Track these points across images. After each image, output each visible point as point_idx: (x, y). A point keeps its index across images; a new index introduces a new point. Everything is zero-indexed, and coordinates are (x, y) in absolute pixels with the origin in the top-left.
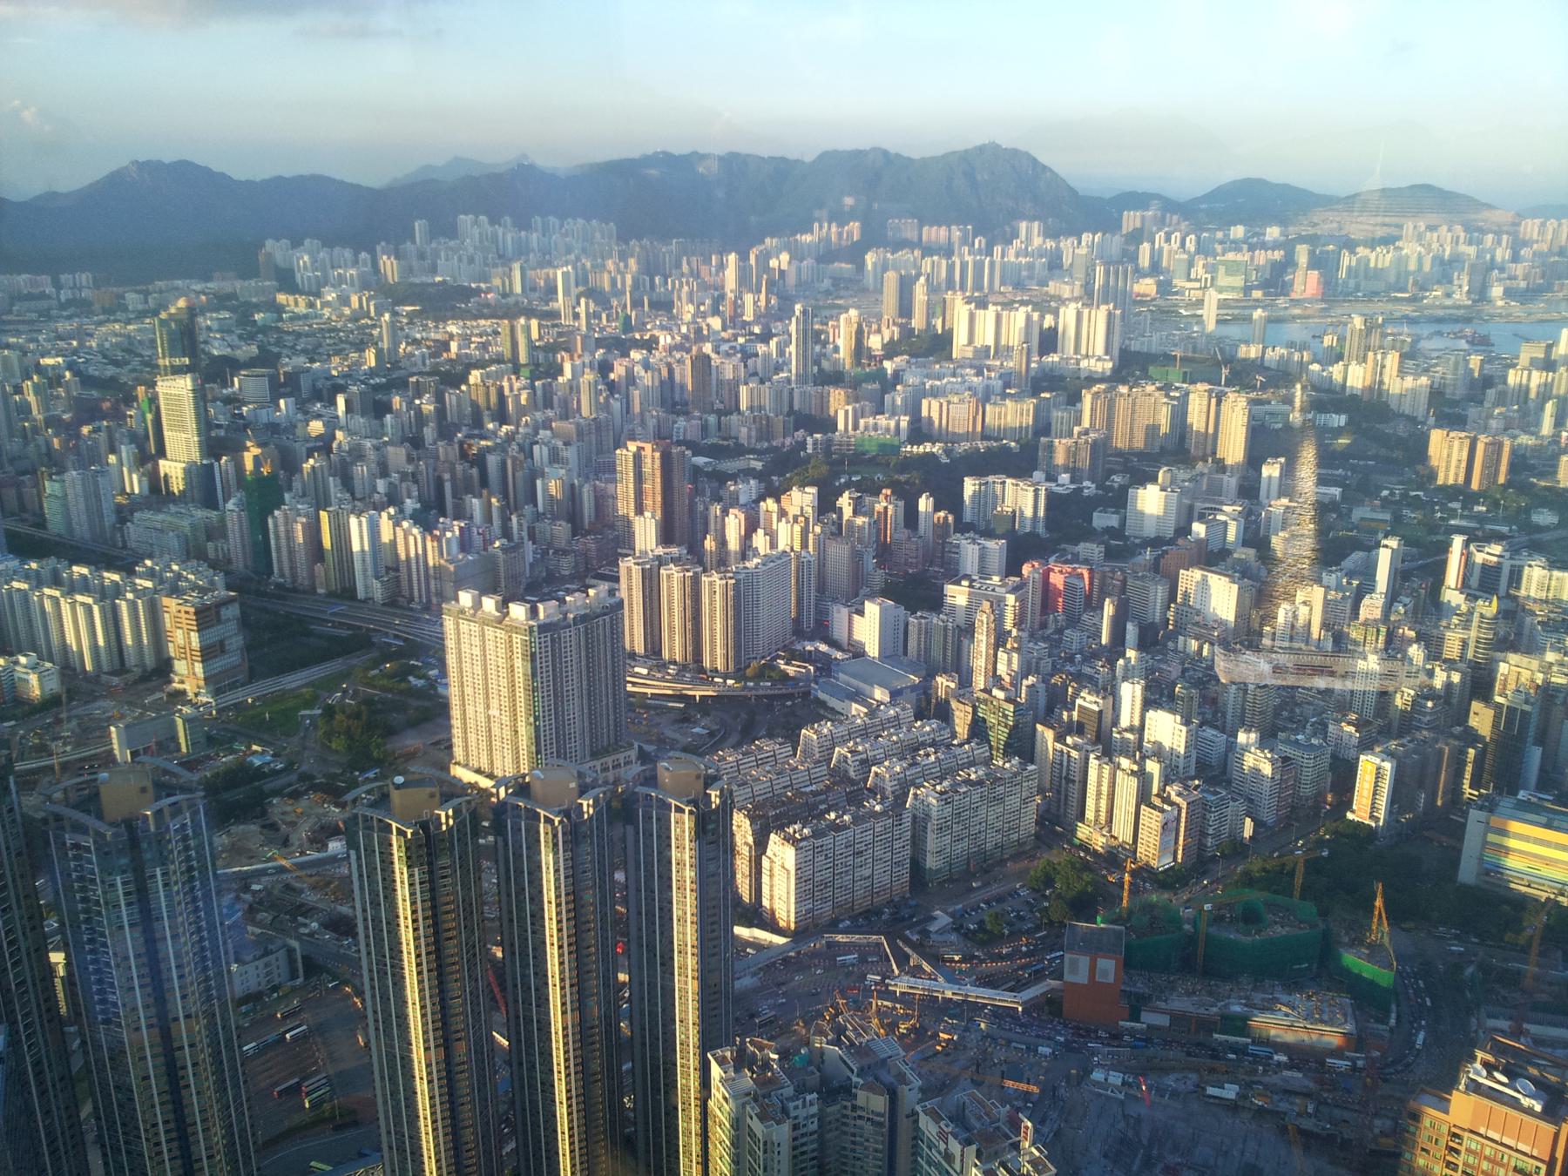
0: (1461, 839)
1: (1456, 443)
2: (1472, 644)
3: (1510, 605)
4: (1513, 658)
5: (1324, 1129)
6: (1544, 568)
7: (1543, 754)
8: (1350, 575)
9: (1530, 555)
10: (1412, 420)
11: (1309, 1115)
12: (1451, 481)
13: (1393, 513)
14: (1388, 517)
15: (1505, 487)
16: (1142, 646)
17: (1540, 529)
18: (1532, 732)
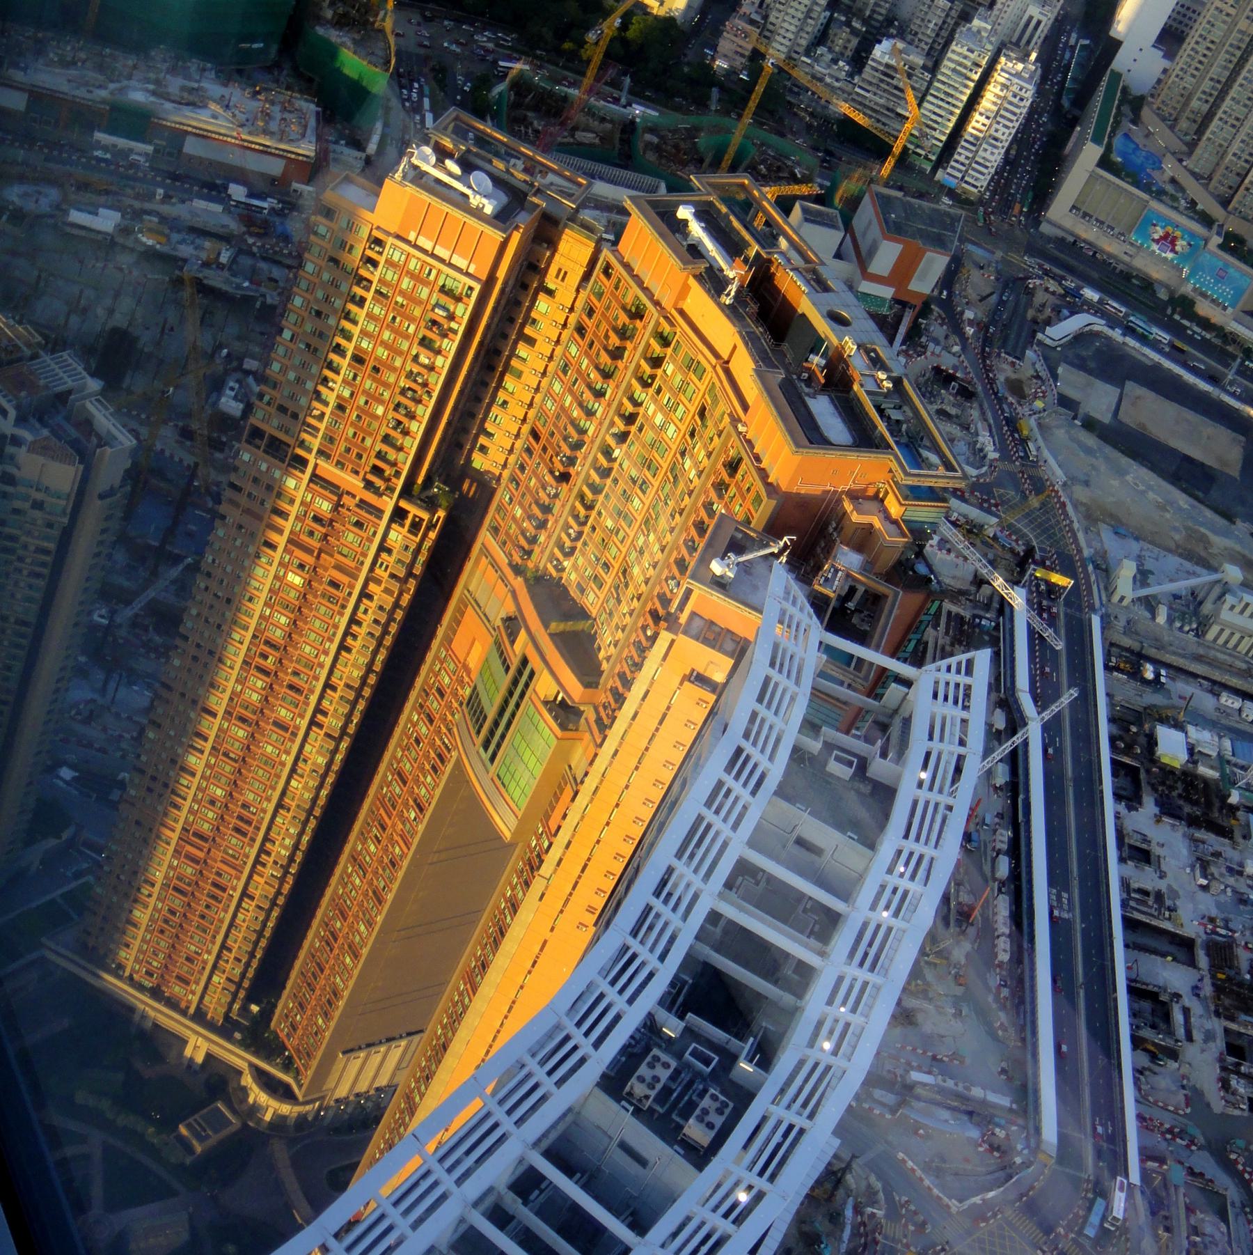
5: (239, 287)
11: (221, 267)
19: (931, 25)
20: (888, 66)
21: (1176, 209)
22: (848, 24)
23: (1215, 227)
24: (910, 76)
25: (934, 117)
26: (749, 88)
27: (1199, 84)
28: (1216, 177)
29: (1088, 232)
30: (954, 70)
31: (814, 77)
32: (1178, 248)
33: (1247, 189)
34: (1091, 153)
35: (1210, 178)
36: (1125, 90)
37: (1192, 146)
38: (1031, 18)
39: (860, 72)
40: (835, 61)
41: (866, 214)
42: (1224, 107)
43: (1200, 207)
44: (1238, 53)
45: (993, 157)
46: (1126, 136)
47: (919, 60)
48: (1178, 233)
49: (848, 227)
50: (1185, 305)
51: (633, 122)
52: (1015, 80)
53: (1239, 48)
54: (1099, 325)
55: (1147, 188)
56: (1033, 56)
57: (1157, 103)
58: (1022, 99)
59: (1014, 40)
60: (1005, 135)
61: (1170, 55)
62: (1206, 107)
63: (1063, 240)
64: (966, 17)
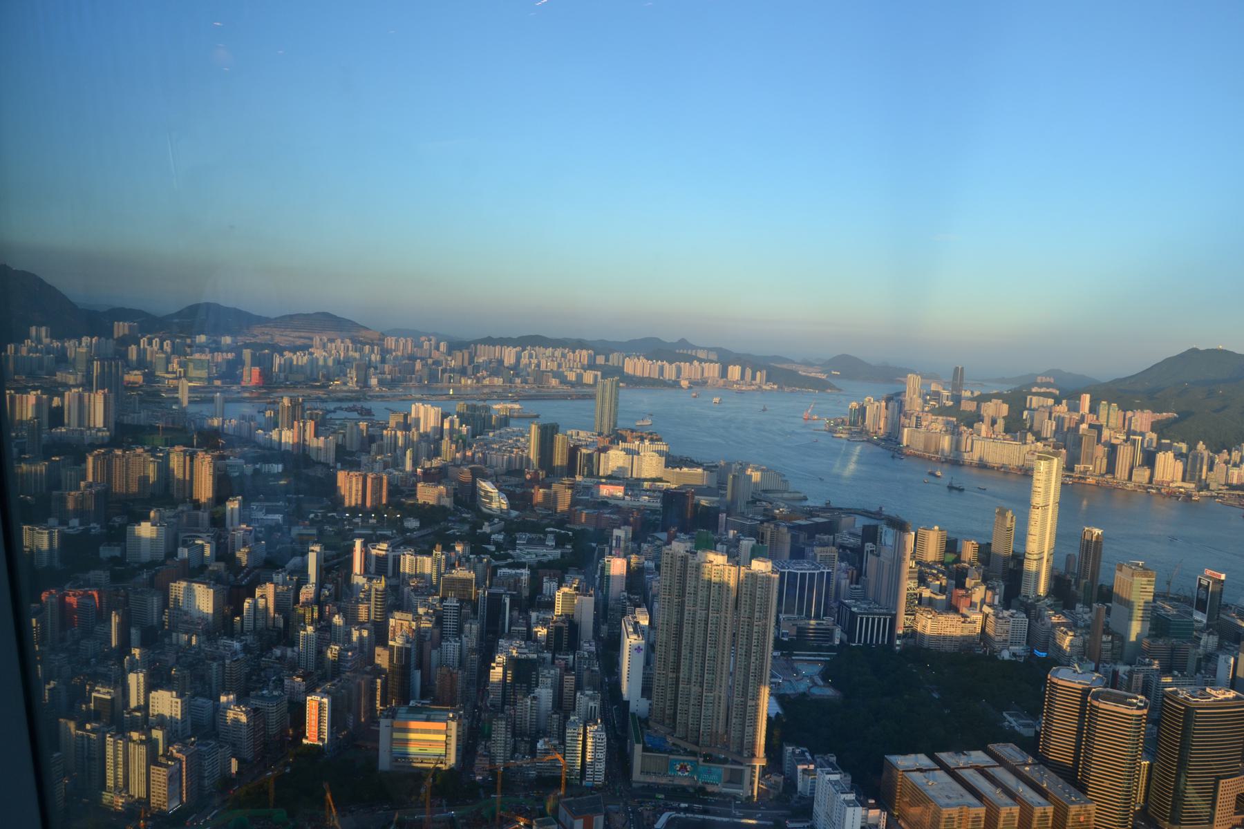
0: (377, 740)
1: (354, 479)
2: (372, 609)
3: (394, 582)
4: (398, 615)
7: (421, 674)
8: (291, 573)
9: (405, 548)
10: (326, 465)
12: (353, 503)
13: (318, 529)
14: (314, 531)
15: (387, 505)
16: (143, 644)
17: (408, 530)
18: (413, 659)
20: (545, 749)
21: (680, 755)
22: (523, 740)
24: (555, 750)
26: (495, 782)
28: (689, 735)
29: (652, 779)
31: (518, 766)
34: (638, 748)
35: (687, 737)
36: (639, 718)
37: (674, 728)
39: (535, 757)
40: (524, 757)
41: (563, 811)
42: (679, 708)
45: (601, 766)
48: (686, 763)
49: (558, 822)
50: (702, 790)
51: (452, 817)
54: (674, 814)
55: (665, 752)
56: (599, 721)
60: (602, 755)
61: (649, 698)
63: (643, 787)
64: (567, 718)
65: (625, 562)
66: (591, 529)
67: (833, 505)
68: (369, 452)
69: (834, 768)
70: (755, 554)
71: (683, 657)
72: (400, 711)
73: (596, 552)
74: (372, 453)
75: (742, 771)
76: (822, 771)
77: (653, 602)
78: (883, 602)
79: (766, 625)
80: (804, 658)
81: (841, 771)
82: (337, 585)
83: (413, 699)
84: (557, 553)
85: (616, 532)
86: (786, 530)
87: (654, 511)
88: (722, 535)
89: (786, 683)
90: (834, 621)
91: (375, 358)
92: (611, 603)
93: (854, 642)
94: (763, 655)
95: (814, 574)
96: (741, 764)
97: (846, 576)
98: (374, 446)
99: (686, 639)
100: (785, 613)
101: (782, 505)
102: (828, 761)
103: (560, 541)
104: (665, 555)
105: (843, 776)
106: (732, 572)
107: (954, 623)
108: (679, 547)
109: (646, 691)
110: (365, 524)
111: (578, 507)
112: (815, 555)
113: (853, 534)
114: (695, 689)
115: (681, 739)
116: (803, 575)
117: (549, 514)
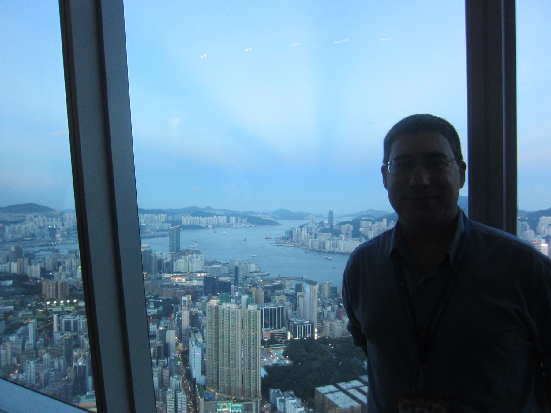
1: (51, 285)
3: (75, 334)
4: (78, 350)
6: (83, 319)
10: (36, 279)
12: (51, 297)
14: (31, 313)
19: (161, 395)
21: (222, 401)
23: (231, 400)
24: (162, 407)
25: (170, 411)
27: (213, 377)
30: (170, 401)
32: (227, 407)
33: (232, 389)
34: (202, 400)
35: (225, 392)
36: (201, 386)
37: (218, 388)
38: (178, 383)
43: (226, 397)
44: (216, 368)
46: (206, 393)
47: (162, 403)
52: (181, 396)
53: (216, 367)
56: (182, 390)
57: (208, 385)
58: (184, 398)
59: (177, 388)
60: (185, 406)
61: (205, 375)
62: (216, 380)
64: (166, 390)
65: (189, 312)
66: (171, 298)
67: (281, 276)
68: (58, 271)
69: (293, 397)
70: (249, 302)
71: (219, 354)
72: (82, 398)
73: (174, 309)
74: (60, 271)
75: (251, 404)
76: (288, 399)
77: (203, 330)
78: (308, 319)
79: (256, 334)
80: (275, 347)
81: (296, 398)
82: (45, 338)
83: (88, 391)
84: (156, 311)
85: (183, 298)
86: (261, 290)
87: (200, 287)
88: (233, 294)
89: (268, 360)
90: (286, 329)
91: (59, 224)
92: (183, 332)
93: (296, 338)
94: (256, 349)
95: (276, 309)
96: (251, 401)
97: (290, 308)
98: (61, 268)
99: (220, 345)
100: (265, 327)
101: (259, 278)
102: (290, 394)
103: (157, 305)
104: (207, 307)
105: (297, 400)
106: (239, 311)
107: (339, 324)
108: (214, 302)
109: (204, 372)
110: (57, 306)
111: (164, 288)
112: (276, 300)
113: (291, 289)
114: (226, 368)
115: (222, 393)
116: (271, 310)
117: (150, 293)
